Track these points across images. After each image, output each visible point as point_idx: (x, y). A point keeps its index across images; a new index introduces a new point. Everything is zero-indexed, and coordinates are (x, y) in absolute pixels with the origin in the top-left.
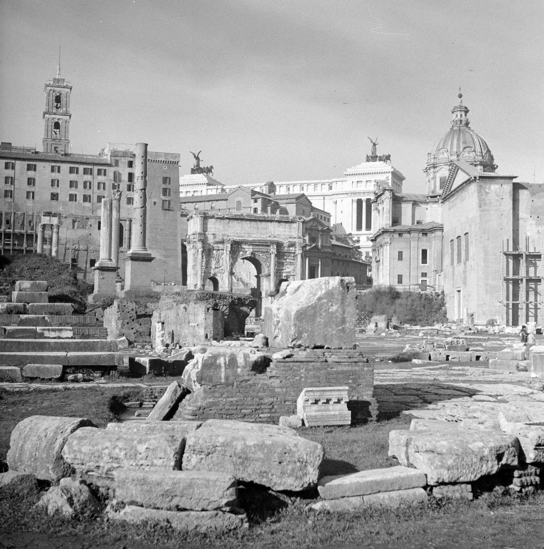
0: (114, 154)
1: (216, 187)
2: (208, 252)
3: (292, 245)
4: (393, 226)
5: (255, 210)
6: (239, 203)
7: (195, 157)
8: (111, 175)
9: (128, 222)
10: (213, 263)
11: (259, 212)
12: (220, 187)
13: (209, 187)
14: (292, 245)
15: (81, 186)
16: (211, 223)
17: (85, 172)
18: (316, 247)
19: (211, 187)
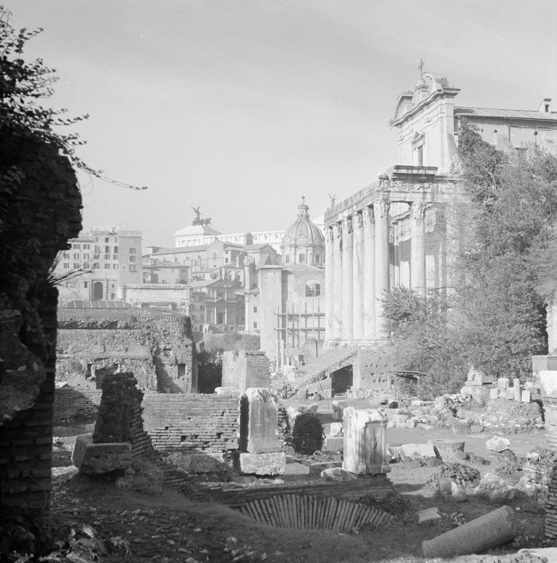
0: (95, 233)
1: (210, 236)
3: (183, 304)
4: (250, 289)
5: (227, 260)
6: (215, 254)
7: (196, 211)
8: (93, 249)
9: (105, 281)
11: (229, 261)
12: (213, 236)
13: (205, 237)
14: (183, 304)
16: (129, 293)
18: (222, 300)
19: (207, 236)
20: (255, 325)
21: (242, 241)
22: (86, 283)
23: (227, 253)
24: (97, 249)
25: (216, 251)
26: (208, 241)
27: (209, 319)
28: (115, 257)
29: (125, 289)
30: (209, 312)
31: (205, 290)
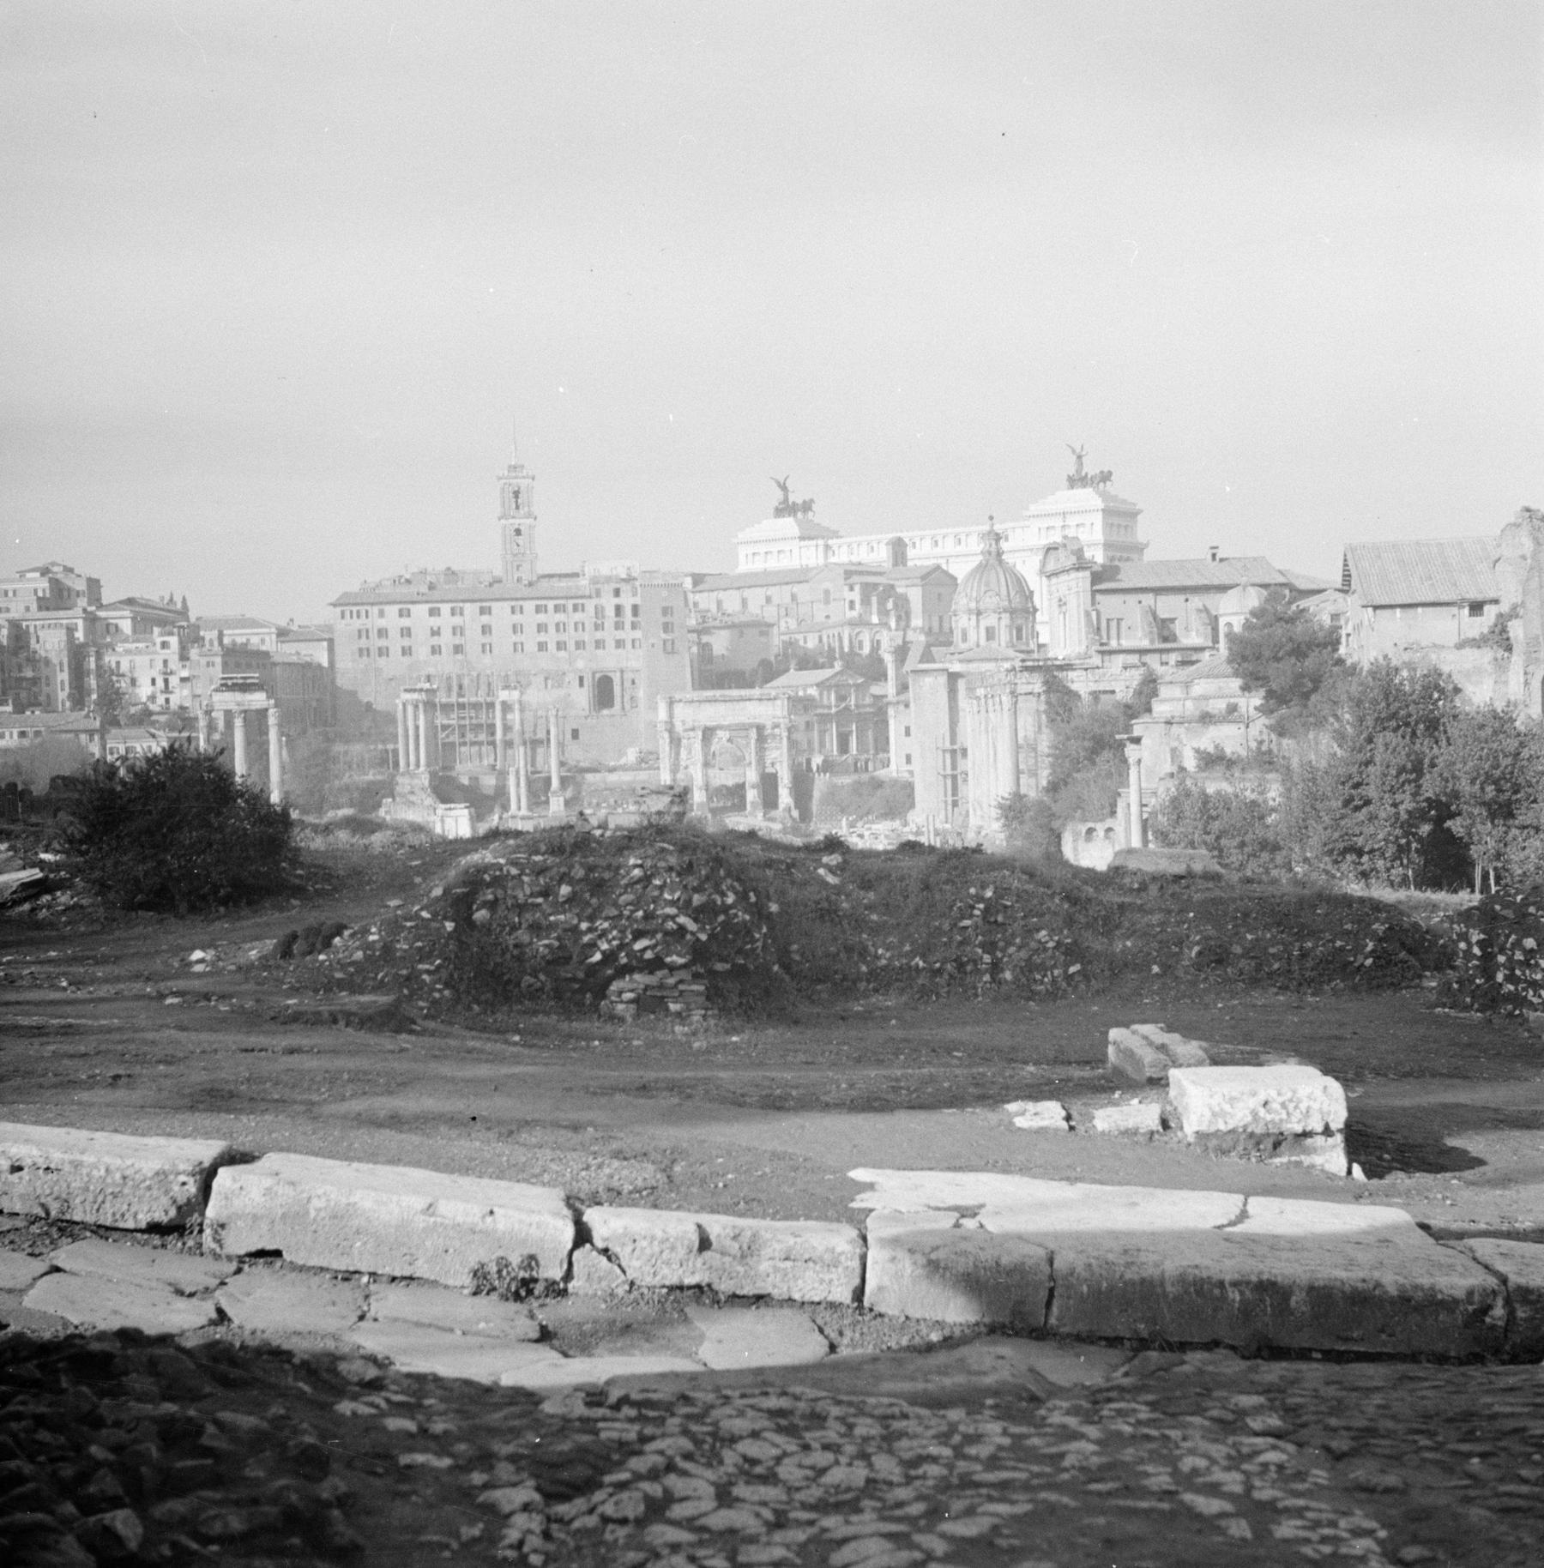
0: (595, 581)
1: (814, 542)
2: (676, 742)
3: (776, 726)
5: (852, 603)
7: (779, 485)
8: (590, 609)
10: (683, 754)
11: (858, 606)
12: (821, 542)
13: (803, 543)
14: (776, 726)
15: (552, 629)
16: (679, 709)
17: (557, 609)
18: (847, 708)
19: (806, 543)
20: (908, 759)
21: (881, 555)
22: (581, 679)
23: (852, 589)
24: (599, 611)
25: (827, 585)
26: (809, 556)
27: (822, 744)
28: (634, 626)
29: (671, 703)
30: (822, 733)
31: (813, 692)
